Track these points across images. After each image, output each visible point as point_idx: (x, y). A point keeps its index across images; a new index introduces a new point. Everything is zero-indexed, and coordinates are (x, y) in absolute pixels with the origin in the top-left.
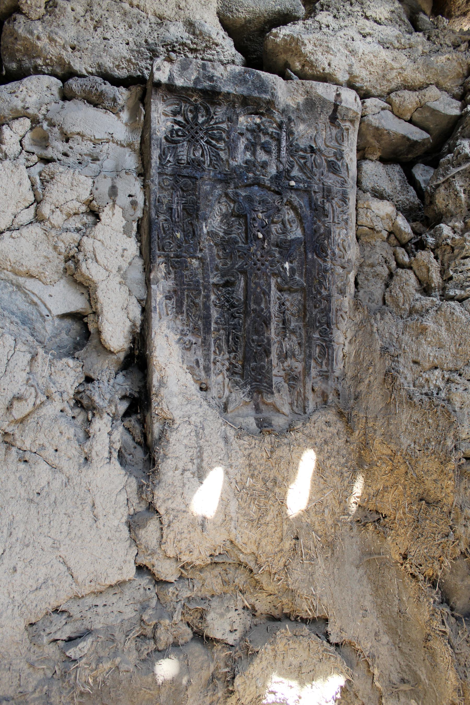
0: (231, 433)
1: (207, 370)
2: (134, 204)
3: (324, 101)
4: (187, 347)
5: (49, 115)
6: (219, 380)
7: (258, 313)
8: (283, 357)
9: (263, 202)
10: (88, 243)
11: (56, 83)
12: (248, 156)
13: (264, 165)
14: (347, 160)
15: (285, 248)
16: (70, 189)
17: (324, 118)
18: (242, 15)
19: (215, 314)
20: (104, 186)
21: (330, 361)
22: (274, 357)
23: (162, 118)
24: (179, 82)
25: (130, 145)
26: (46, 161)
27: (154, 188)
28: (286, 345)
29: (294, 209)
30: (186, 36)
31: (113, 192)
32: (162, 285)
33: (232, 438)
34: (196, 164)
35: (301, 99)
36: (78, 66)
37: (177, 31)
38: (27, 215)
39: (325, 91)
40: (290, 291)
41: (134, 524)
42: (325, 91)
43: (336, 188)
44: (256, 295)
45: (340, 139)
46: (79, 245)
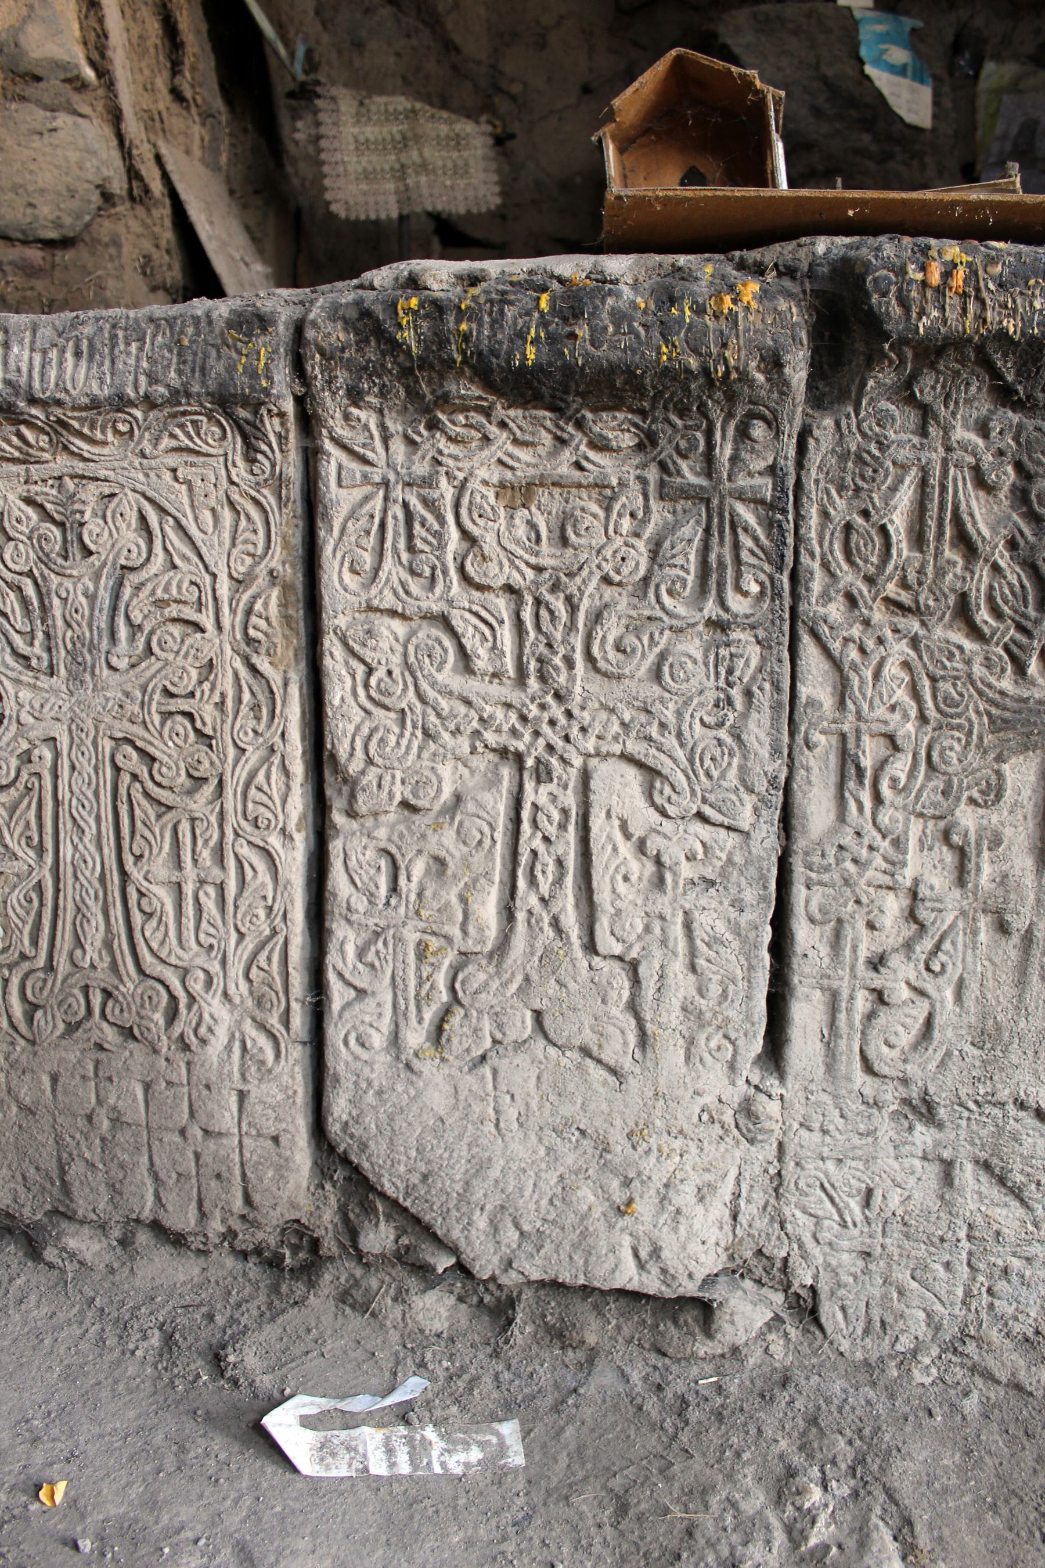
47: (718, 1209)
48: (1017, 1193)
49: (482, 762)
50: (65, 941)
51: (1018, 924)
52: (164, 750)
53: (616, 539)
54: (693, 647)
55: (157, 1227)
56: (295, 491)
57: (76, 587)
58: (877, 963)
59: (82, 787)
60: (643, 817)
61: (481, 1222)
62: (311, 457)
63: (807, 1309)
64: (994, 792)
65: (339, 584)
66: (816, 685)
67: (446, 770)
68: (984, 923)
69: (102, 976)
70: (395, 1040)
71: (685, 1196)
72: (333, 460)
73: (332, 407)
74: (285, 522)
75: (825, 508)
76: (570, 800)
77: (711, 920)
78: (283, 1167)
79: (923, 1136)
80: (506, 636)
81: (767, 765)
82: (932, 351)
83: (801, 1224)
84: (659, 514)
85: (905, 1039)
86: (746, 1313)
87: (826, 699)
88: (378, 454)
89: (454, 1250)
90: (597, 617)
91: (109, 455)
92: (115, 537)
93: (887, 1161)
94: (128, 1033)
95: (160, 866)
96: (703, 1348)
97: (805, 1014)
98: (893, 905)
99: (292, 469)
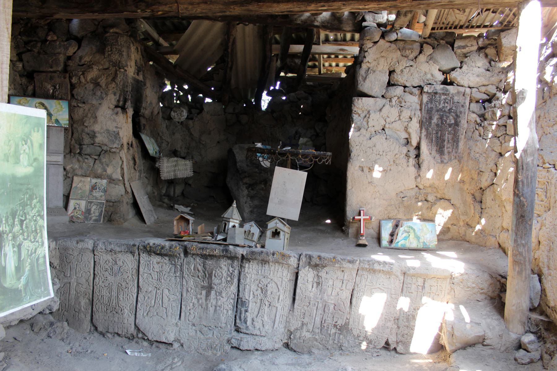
4: (428, 146)
6: (434, 152)
9: (446, 115)
11: (403, 88)
13: (447, 107)
15: (450, 125)
16: (406, 114)
17: (462, 95)
19: (434, 139)
20: (413, 113)
21: (458, 149)
23: (425, 98)
24: (429, 91)
30: (431, 78)
31: (415, 114)
32: (424, 133)
34: (432, 108)
35: (456, 91)
36: (407, 85)
37: (429, 76)
38: (398, 119)
41: (416, 178)
42: (462, 89)
43: (463, 111)
44: (443, 135)
45: (465, 99)
47: (173, 334)
51: (204, 306)
52: (123, 284)
54: (173, 278)
59: (115, 288)
60: (168, 294)
62: (139, 258)
63: (182, 345)
64: (201, 294)
65: (141, 269)
66: (184, 283)
69: (115, 307)
70: (143, 314)
71: (170, 332)
72: (141, 258)
73: (141, 254)
74: (137, 263)
75: (185, 267)
77: (174, 304)
78: (131, 327)
79: (194, 328)
80: (156, 276)
81: (179, 290)
82: (193, 254)
83: (182, 336)
86: (176, 345)
89: (146, 336)
91: (120, 255)
92: (120, 263)
95: (122, 296)
96: (171, 348)
97: (183, 314)
98: (191, 304)
99: (138, 259)
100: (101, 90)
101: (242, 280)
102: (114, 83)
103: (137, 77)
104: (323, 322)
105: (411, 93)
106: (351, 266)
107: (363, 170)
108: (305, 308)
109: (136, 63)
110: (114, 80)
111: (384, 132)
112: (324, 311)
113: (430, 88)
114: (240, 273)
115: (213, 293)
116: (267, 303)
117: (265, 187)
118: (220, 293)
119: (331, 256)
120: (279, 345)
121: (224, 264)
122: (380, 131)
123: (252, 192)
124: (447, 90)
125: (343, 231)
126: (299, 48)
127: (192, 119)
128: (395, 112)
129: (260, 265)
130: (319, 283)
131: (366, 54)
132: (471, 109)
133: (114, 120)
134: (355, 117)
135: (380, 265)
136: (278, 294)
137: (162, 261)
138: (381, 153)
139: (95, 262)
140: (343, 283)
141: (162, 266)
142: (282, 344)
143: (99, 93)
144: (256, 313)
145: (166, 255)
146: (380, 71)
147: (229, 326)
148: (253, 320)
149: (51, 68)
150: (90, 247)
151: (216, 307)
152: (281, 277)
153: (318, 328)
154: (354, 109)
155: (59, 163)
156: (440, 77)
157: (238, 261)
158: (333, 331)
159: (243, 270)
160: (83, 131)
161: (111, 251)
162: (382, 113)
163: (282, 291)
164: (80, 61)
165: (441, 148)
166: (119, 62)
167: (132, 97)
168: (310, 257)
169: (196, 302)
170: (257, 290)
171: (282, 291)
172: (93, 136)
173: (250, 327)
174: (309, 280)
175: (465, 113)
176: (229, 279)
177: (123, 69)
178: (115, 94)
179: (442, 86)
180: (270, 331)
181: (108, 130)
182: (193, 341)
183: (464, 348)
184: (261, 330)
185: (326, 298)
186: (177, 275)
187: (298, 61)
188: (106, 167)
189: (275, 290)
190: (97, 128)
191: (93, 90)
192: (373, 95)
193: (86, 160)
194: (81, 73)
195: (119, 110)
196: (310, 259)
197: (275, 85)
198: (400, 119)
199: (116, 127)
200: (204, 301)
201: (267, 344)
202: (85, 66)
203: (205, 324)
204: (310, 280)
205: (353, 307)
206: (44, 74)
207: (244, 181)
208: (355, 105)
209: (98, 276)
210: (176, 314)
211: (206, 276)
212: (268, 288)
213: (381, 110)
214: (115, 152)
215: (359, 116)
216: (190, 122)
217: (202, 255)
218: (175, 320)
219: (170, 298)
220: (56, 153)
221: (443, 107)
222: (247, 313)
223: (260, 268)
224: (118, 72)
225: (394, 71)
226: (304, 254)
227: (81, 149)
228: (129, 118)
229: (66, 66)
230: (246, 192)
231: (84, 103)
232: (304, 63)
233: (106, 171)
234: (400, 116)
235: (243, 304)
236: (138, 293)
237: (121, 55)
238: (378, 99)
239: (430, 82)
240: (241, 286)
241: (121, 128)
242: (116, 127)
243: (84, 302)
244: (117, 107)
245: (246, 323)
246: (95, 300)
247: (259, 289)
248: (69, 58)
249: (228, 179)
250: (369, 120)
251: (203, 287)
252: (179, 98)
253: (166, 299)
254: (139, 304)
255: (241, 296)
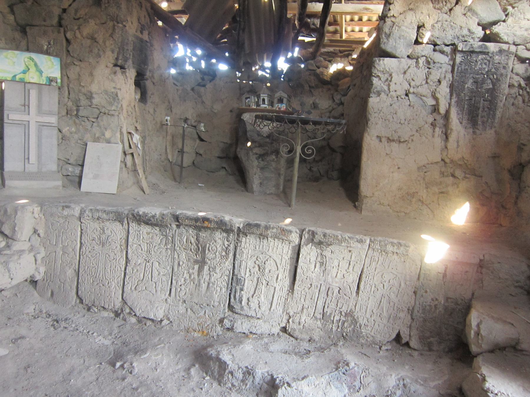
0: (466, 133)
1: (462, 119)
2: (449, 80)
3: (504, 50)
4: (458, 114)
5: (431, 57)
6: (464, 122)
7: (477, 107)
8: (482, 117)
10: (438, 90)
11: (432, 46)
12: (480, 66)
13: (484, 69)
14: (509, 65)
18: (484, 22)
19: (466, 106)
20: (443, 76)
22: (479, 117)
24: (464, 50)
25: (450, 65)
26: (429, 68)
27: (455, 76)
28: (483, 114)
29: (490, 79)
30: (468, 33)
31: (445, 77)
32: (454, 99)
33: (466, 136)
35: (497, 50)
36: (438, 43)
37: (465, 32)
38: (424, 82)
39: (505, 47)
40: (486, 101)
41: (442, 150)
42: (505, 47)
43: (505, 73)
46: (436, 90)
47: (163, 310)
48: (194, 313)
49: (143, 260)
50: (98, 274)
53: (157, 240)
55: (103, 307)
56: (127, 230)
57: (104, 237)
58: (181, 285)
61: (138, 309)
64: (194, 268)
65: (130, 240)
67: (139, 260)
68: (192, 282)
70: (131, 289)
71: (159, 308)
73: (131, 224)
75: (177, 238)
76: (151, 265)
77: (164, 278)
84: (162, 237)
85: (183, 294)
87: (177, 258)
88: (135, 228)
89: (134, 312)
90: (155, 247)
92: (108, 232)
93: (181, 307)
94: (103, 285)
97: (173, 290)
98: (183, 279)
99: (126, 227)
100: (99, 46)
101: (237, 256)
102: (112, 39)
103: (140, 36)
104: (326, 306)
105: (442, 52)
106: (359, 245)
107: (381, 141)
108: (306, 289)
109: (139, 20)
110: (111, 36)
111: (407, 98)
112: (327, 295)
113: (466, 45)
114: (236, 248)
115: (206, 268)
116: (264, 282)
117: (277, 157)
118: (214, 268)
119: (339, 233)
120: (276, 330)
121: (219, 236)
122: (403, 97)
123: (262, 163)
124: (486, 47)
125: (355, 206)
126: (319, 7)
127: (204, 86)
128: (420, 74)
129: (258, 240)
130: (323, 263)
131: (391, 7)
132: (514, 71)
133: (112, 80)
134: (375, 81)
135: (394, 246)
136: (277, 272)
137: (152, 231)
138: (402, 122)
139: (82, 230)
140: (349, 264)
141: (152, 237)
142: (279, 327)
143: (96, 51)
144: (252, 293)
145: (156, 225)
146: (406, 27)
147: (222, 305)
148: (248, 299)
149: (45, 21)
150: (77, 214)
151: (209, 284)
152: (281, 254)
153: (320, 314)
154: (375, 71)
155: (53, 125)
156: (480, 33)
157: (234, 235)
158: (337, 318)
159: (239, 244)
160: (80, 91)
161: (98, 219)
162: (406, 76)
163: (281, 270)
164: (76, 14)
165: (474, 117)
166: (117, 16)
167: (133, 56)
168: (313, 234)
169: (188, 277)
170: (254, 267)
171: (281, 270)
172: (90, 97)
173: (245, 308)
174: (311, 259)
175: (506, 76)
176: (224, 253)
177: (122, 24)
178: (113, 52)
179: (481, 43)
180: (267, 313)
181: (106, 91)
182: (183, 320)
183: (492, 351)
184: (257, 312)
185: (330, 280)
186: (168, 247)
187: (317, 22)
188: (105, 131)
189: (274, 268)
190: (94, 88)
191: (90, 47)
192: (397, 55)
193: (83, 123)
194: (76, 28)
195: (118, 69)
196: (314, 236)
197: (293, 52)
198: (427, 83)
199: (114, 88)
200: (196, 277)
201: (263, 327)
202: (81, 20)
203: (196, 302)
204: (313, 259)
205: (360, 292)
206: (37, 28)
207: (254, 152)
208: (375, 67)
209: (85, 245)
210: (166, 289)
211: (199, 249)
212: (266, 266)
213: (405, 73)
214: (113, 115)
215: (380, 79)
216: (202, 89)
217: (194, 226)
218: (164, 296)
219: (160, 271)
220: (50, 113)
221: (480, 69)
222: (242, 292)
223: (258, 243)
224: (116, 27)
225: (423, 26)
226: (307, 230)
227: (78, 110)
228: (129, 80)
229: (60, 18)
230: (256, 163)
231: (81, 61)
232: (323, 24)
233: (104, 135)
234: (427, 78)
235: (238, 281)
236: (126, 265)
237: (119, 7)
238: (402, 60)
239: (466, 39)
240: (236, 262)
241: (120, 89)
242: (114, 88)
243: (70, 272)
244: (116, 65)
245: (241, 303)
246: (81, 271)
247: (256, 266)
248: (64, 10)
249: (238, 150)
250: (391, 84)
251: (196, 262)
252: (191, 63)
253: (155, 273)
254: (127, 277)
255: (236, 272)
